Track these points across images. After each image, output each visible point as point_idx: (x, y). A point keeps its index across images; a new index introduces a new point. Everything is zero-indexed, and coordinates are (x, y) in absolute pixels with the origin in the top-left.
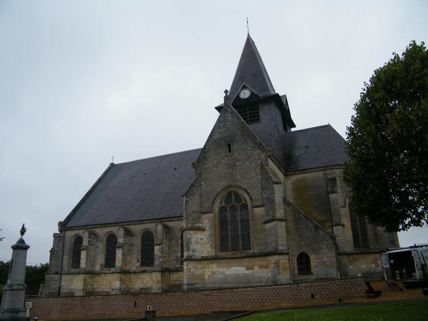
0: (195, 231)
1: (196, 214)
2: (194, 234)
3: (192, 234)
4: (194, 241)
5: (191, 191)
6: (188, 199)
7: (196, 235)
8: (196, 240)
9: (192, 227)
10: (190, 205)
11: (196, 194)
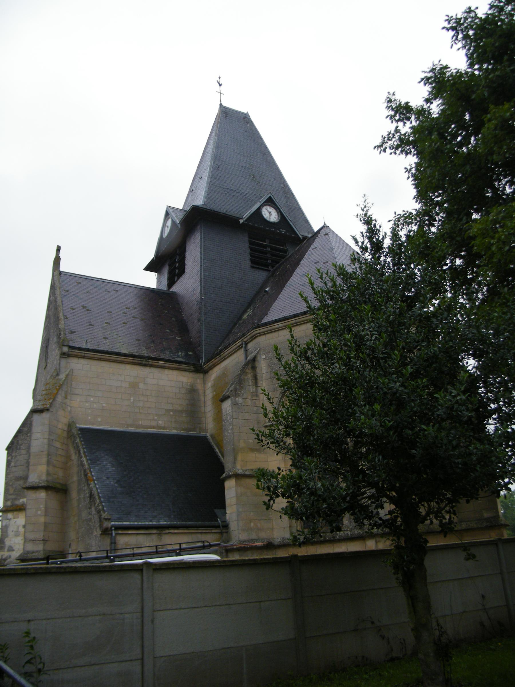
0: (15, 513)
1: (19, 483)
2: (14, 518)
3: (10, 519)
4: (13, 531)
5: (16, 442)
6: (238, 387)
7: (15, 520)
8: (15, 529)
9: (12, 506)
10: (12, 467)
11: (23, 445)
